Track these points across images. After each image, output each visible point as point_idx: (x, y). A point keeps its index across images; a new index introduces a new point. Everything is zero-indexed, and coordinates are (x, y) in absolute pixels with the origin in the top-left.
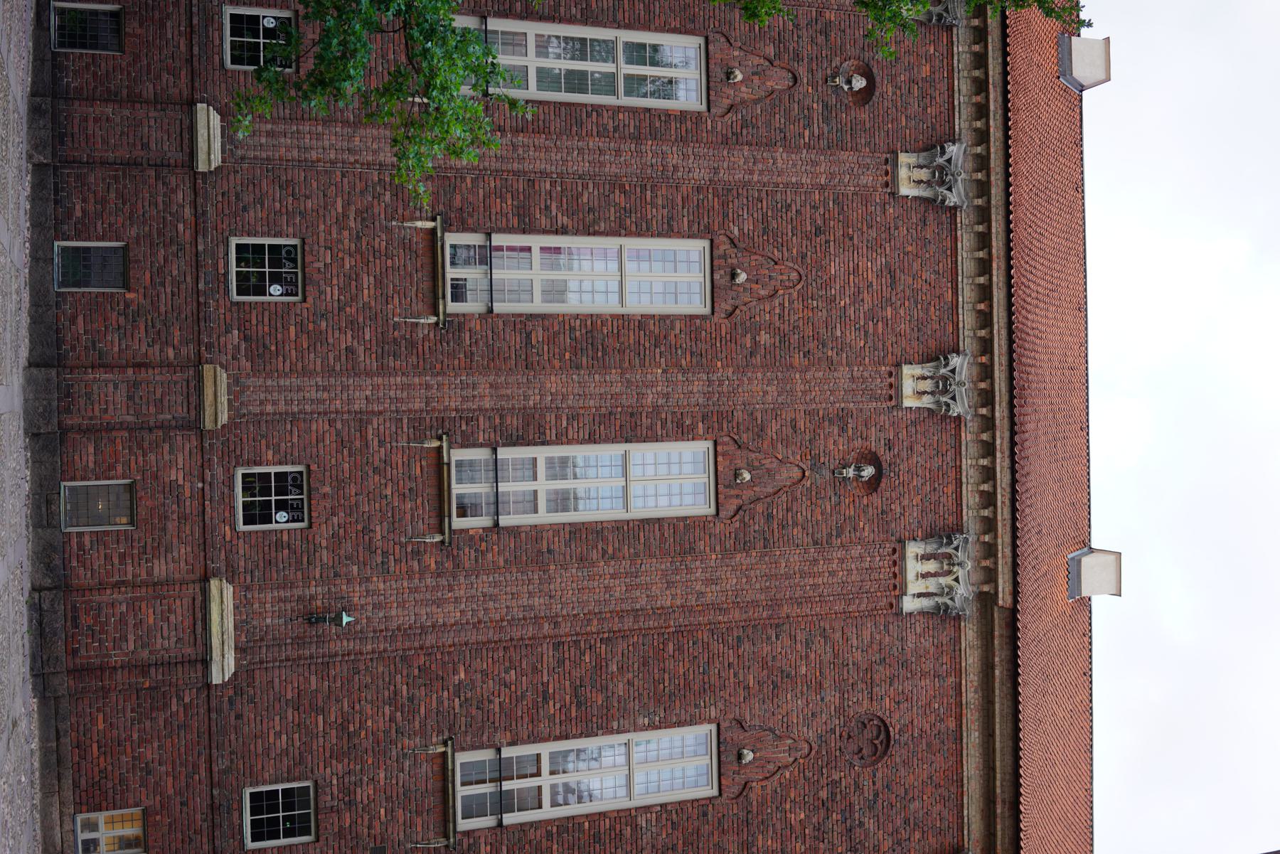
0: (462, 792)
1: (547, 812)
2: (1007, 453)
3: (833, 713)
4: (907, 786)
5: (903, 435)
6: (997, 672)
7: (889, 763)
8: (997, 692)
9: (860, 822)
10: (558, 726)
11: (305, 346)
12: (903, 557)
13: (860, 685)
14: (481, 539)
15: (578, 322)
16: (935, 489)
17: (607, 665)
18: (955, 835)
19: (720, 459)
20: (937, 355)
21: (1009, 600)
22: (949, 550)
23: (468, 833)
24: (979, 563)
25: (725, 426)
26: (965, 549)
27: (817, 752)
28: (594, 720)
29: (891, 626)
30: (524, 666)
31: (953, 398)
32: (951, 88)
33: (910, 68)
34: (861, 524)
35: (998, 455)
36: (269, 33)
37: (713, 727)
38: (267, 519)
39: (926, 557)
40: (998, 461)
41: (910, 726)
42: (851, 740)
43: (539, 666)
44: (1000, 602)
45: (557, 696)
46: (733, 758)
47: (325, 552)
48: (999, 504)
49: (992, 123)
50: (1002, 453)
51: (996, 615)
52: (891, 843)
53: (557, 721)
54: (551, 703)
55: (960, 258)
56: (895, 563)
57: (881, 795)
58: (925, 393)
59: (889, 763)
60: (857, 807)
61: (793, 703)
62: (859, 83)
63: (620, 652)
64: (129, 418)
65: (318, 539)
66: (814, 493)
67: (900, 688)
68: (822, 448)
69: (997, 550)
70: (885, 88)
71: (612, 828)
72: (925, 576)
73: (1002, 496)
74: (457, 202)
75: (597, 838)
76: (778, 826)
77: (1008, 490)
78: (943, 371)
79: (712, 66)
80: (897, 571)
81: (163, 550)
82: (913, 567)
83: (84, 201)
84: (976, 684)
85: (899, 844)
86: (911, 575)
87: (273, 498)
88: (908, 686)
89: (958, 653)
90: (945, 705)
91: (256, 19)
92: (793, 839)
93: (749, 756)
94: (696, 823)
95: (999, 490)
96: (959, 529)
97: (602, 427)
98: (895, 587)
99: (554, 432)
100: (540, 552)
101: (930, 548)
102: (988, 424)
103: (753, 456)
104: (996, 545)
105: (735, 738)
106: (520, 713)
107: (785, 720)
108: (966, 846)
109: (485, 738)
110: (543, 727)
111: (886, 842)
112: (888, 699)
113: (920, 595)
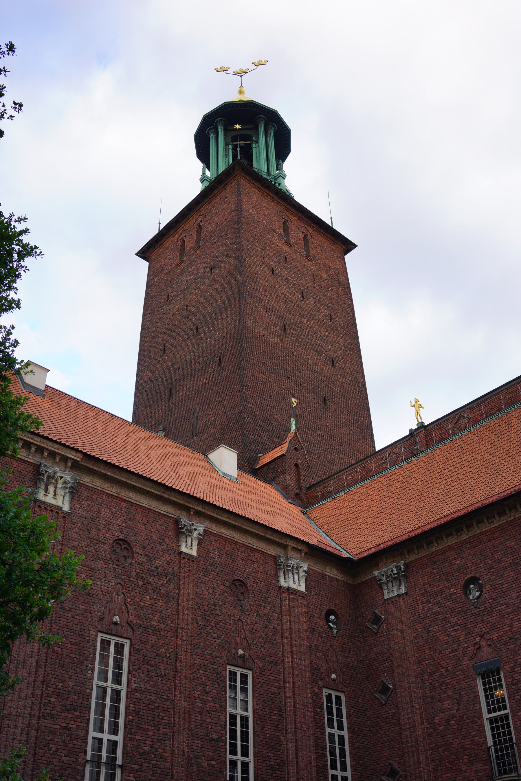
1: (119, 738)
3: (107, 566)
4: (146, 538)
6: (109, 473)
7: (134, 544)
8: (117, 477)
9: (156, 568)
10: (82, 724)
12: (44, 503)
13: (97, 547)
17: (58, 689)
18: (170, 520)
21: (79, 455)
24: (56, 462)
26: (48, 468)
27: (122, 581)
28: (83, 702)
29: (73, 521)
30: (49, 738)
37: (100, 634)
39: (46, 490)
41: (120, 527)
42: (120, 560)
43: (51, 729)
44: (79, 459)
45: (68, 722)
46: (115, 628)
48: (32, 441)
51: (83, 464)
52: (167, 555)
53: (80, 724)
54: (71, 726)
56: (45, 508)
57: (147, 553)
59: (134, 544)
60: (150, 567)
63: (53, 679)
67: (102, 526)
69: (54, 451)
73: (28, 437)
75: (137, 713)
76: (150, 612)
82: (49, 499)
84: (109, 486)
85: (168, 550)
86: (53, 502)
88: (102, 522)
89: (93, 490)
90: (115, 505)
92: (156, 605)
93: (116, 619)
94: (141, 656)
95: (25, 438)
96: (37, 467)
98: (57, 512)
104: (51, 451)
105: (107, 624)
106: (72, 746)
107: (104, 593)
108: (176, 517)
109: (80, 768)
110: (81, 733)
111: (167, 557)
112: (107, 535)
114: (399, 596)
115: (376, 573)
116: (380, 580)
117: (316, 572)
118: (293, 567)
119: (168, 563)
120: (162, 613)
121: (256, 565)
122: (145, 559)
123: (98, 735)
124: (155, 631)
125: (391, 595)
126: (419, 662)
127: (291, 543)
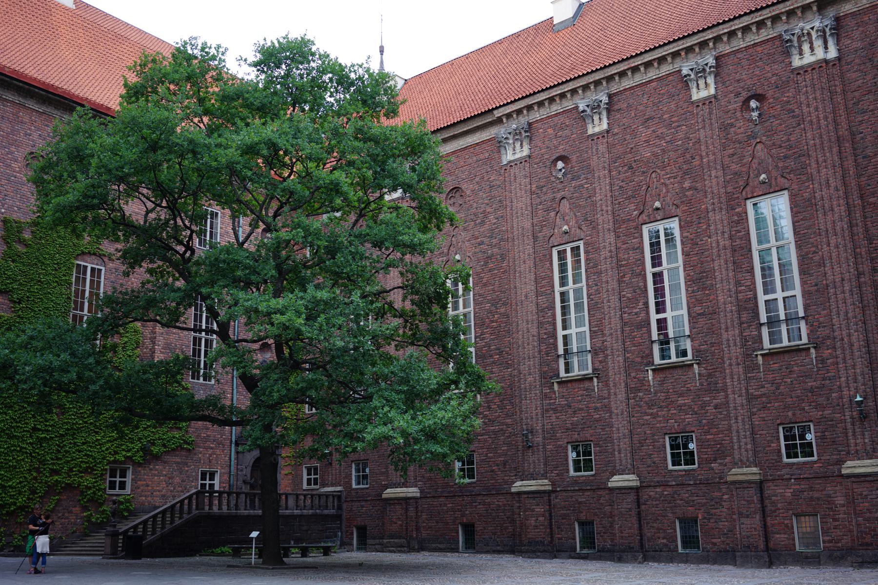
2: (731, 23)
5: (731, 88)
11: (716, 430)
12: (802, 67)
14: (812, 325)
15: (689, 289)
16: (761, 59)
19: (755, 194)
20: (685, 82)
22: (795, 39)
25: (736, 196)
26: (792, 29)
29: (849, 60)
31: (706, 64)
32: (556, 115)
33: (550, 140)
34: (785, 99)
35: (733, 28)
36: (578, 455)
38: (810, 444)
39: (801, 53)
40: (736, 27)
47: (826, 412)
48: (761, 18)
49: (566, 90)
50: (732, 26)
55: (634, 84)
58: (706, 83)
62: (560, 164)
64: (758, 517)
65: (819, 417)
66: (769, 133)
68: (743, 135)
69: (790, 10)
70: (560, 151)
72: (812, 49)
74: (639, 360)
77: (752, 15)
78: (693, 76)
79: (564, 242)
80: (810, 69)
81: (829, 499)
82: (808, 59)
83: (659, 538)
86: (813, 59)
87: (798, 442)
89: (861, 12)
91: (574, 461)
95: (754, 21)
97: (743, 266)
99: (748, 293)
100: (818, 291)
101: (795, 51)
102: (717, 39)
103: (752, 175)
104: (786, 12)
113: (826, 48)
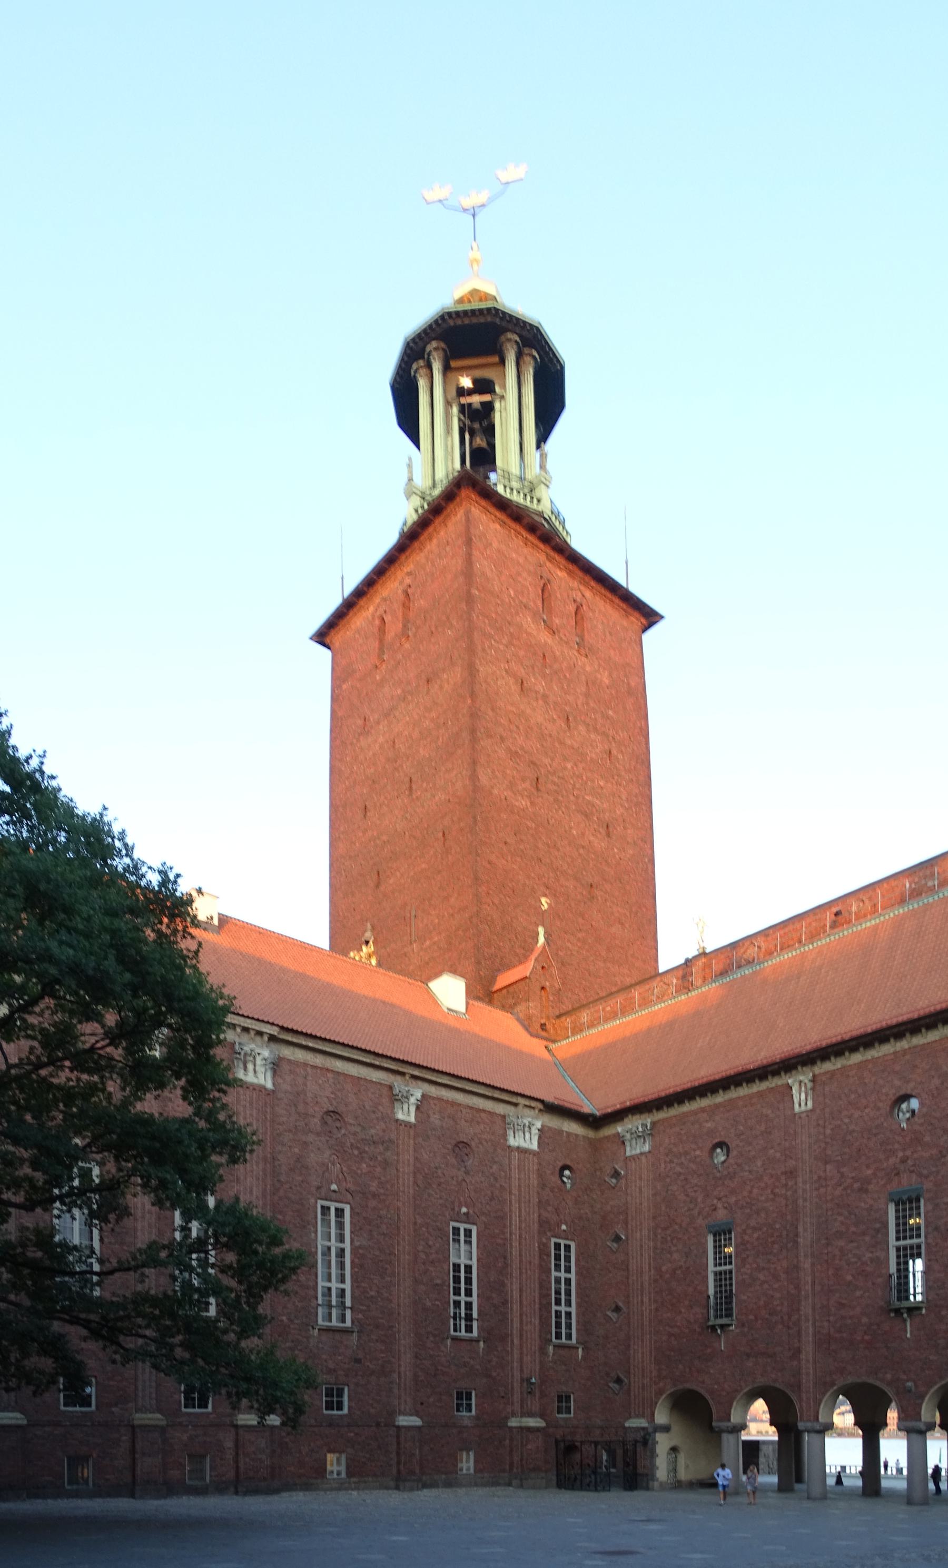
0: (334, 1323)
1: (347, 1286)
23: (353, 1322)
46: (334, 1195)
61: (313, 1158)
71: (358, 1258)
75: (362, 1266)
93: (334, 1187)
114: (641, 1154)
115: (620, 1129)
116: (623, 1137)
117: (550, 1128)
118: (524, 1126)
119: (384, 1131)
120: (380, 1178)
121: (482, 1126)
122: (358, 1129)
123: (328, 1284)
124: (374, 1195)
125: (634, 1152)
126: (654, 1218)
127: (522, 1101)
